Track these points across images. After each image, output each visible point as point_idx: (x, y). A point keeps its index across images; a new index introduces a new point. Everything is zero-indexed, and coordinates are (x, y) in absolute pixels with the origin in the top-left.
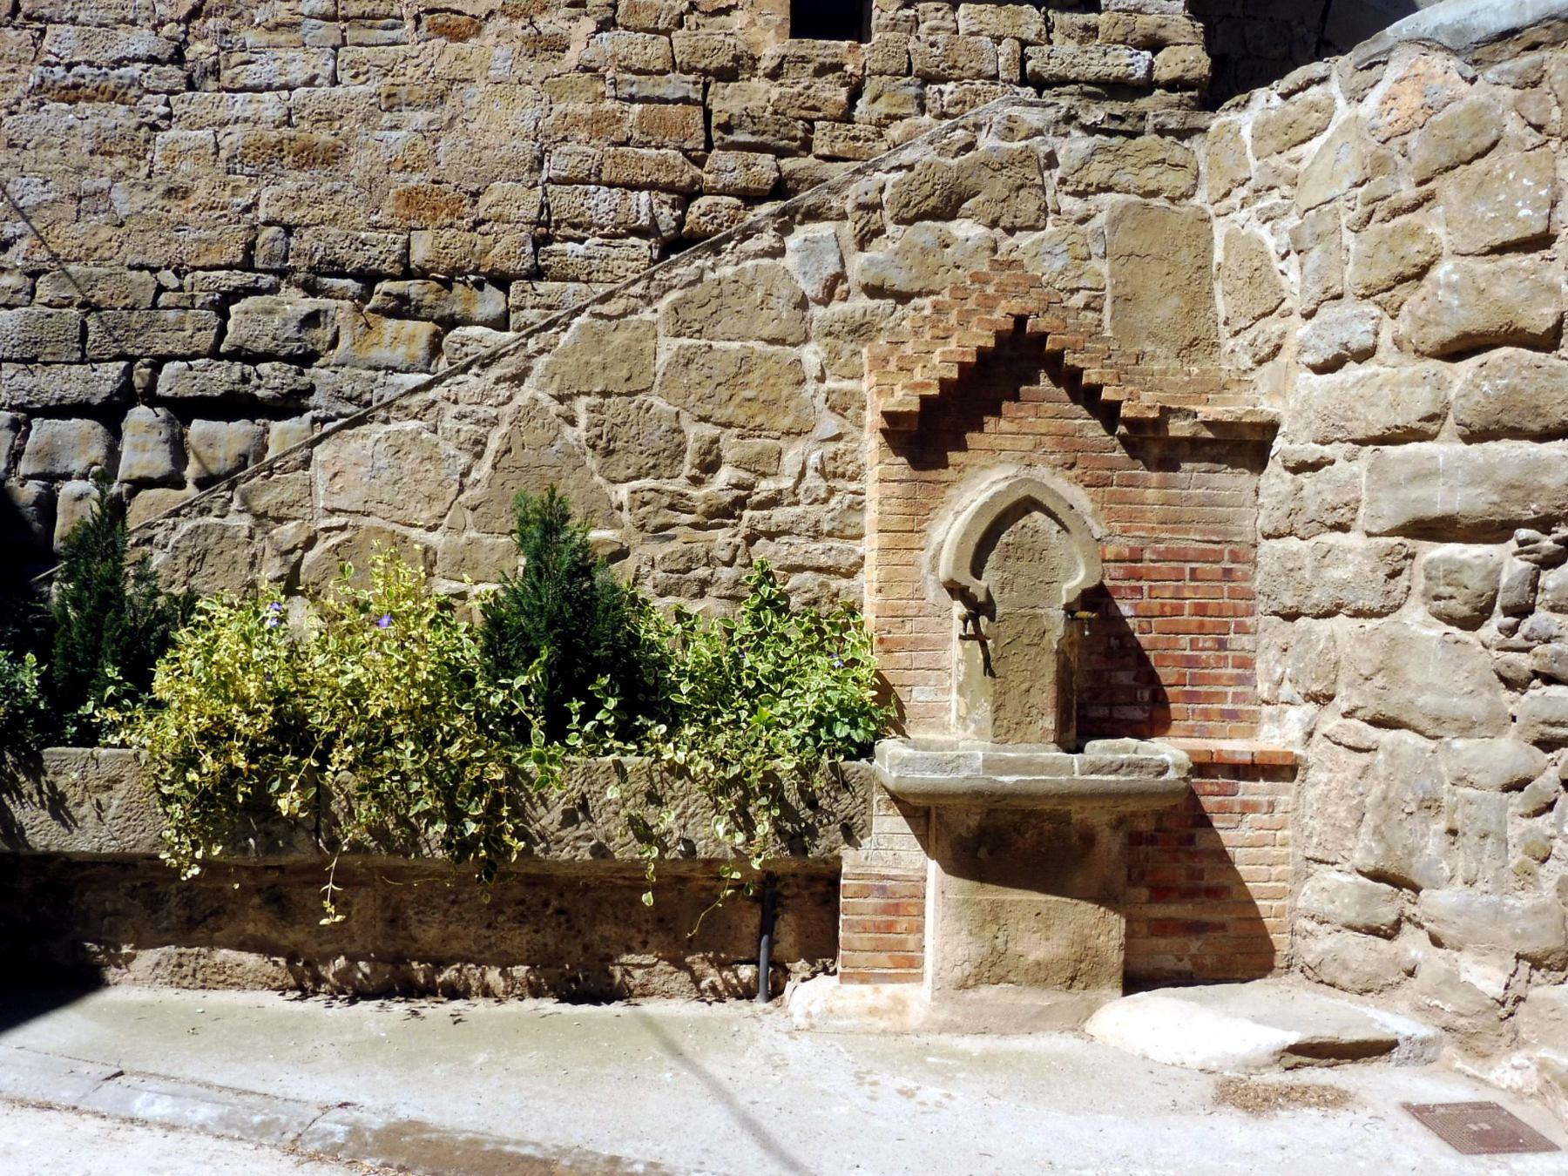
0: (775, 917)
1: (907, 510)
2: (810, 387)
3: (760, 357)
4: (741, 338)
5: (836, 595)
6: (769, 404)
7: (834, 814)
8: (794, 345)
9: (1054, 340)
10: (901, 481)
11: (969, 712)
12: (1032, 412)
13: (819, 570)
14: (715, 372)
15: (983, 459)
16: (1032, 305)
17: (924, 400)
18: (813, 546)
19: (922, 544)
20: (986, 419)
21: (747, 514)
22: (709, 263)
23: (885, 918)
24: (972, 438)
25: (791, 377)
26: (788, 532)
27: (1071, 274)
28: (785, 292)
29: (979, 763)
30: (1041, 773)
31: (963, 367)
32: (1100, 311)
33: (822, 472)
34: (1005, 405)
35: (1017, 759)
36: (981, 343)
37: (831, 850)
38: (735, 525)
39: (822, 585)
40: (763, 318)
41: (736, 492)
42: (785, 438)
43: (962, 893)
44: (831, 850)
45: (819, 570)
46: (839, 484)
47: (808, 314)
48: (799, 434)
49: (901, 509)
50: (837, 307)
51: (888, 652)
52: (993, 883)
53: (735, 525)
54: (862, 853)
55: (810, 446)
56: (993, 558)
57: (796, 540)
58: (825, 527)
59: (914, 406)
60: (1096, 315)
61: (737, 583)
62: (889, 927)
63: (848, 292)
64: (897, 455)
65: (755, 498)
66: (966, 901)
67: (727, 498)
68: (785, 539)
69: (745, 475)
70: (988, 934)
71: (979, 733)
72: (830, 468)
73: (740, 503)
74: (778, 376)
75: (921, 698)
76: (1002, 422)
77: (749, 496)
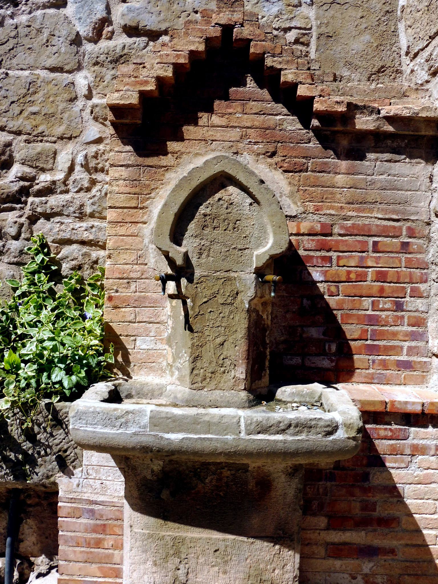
0: (20, 521)
1: (133, 190)
2: (80, 103)
3: (43, 81)
4: (30, 68)
5: (96, 262)
6: (49, 116)
7: (51, 447)
8: (69, 72)
9: (256, 45)
10: (127, 166)
11: (174, 361)
12: (239, 109)
13: (83, 243)
14: (9, 94)
15: (197, 148)
16: (237, 17)
17: (142, 94)
18: (78, 225)
19: (145, 218)
20: (200, 114)
21: (31, 199)
22: (9, 12)
23: (94, 535)
24: (189, 130)
25: (66, 96)
26: (59, 214)
27: (285, 17)
28: (64, 33)
29: (146, 420)
30: (208, 432)
31: (177, 67)
32: (308, 45)
33: (85, 166)
34: (217, 103)
35: (184, 417)
36: (193, 48)
37: (48, 477)
38: (22, 208)
39: (85, 255)
40: (47, 53)
41: (22, 183)
42: (60, 142)
43: (148, 528)
44: (48, 477)
45: (83, 243)
46: (100, 176)
47: (82, 50)
48: (70, 138)
49: (128, 190)
50: (104, 44)
51: (116, 307)
52: (174, 521)
53: (22, 208)
54: (74, 481)
55: (78, 147)
56: (192, 226)
57: (66, 220)
58: (88, 210)
59: (134, 99)
60: (304, 48)
61: (21, 252)
62: (98, 543)
63: (113, 33)
64: (125, 144)
65: (36, 187)
66: (150, 536)
67: (15, 187)
68: (57, 219)
69: (27, 169)
70: (171, 565)
71: (181, 379)
72: (92, 164)
73: (24, 192)
74: (56, 95)
75: (144, 346)
76: (214, 117)
77: (31, 186)
